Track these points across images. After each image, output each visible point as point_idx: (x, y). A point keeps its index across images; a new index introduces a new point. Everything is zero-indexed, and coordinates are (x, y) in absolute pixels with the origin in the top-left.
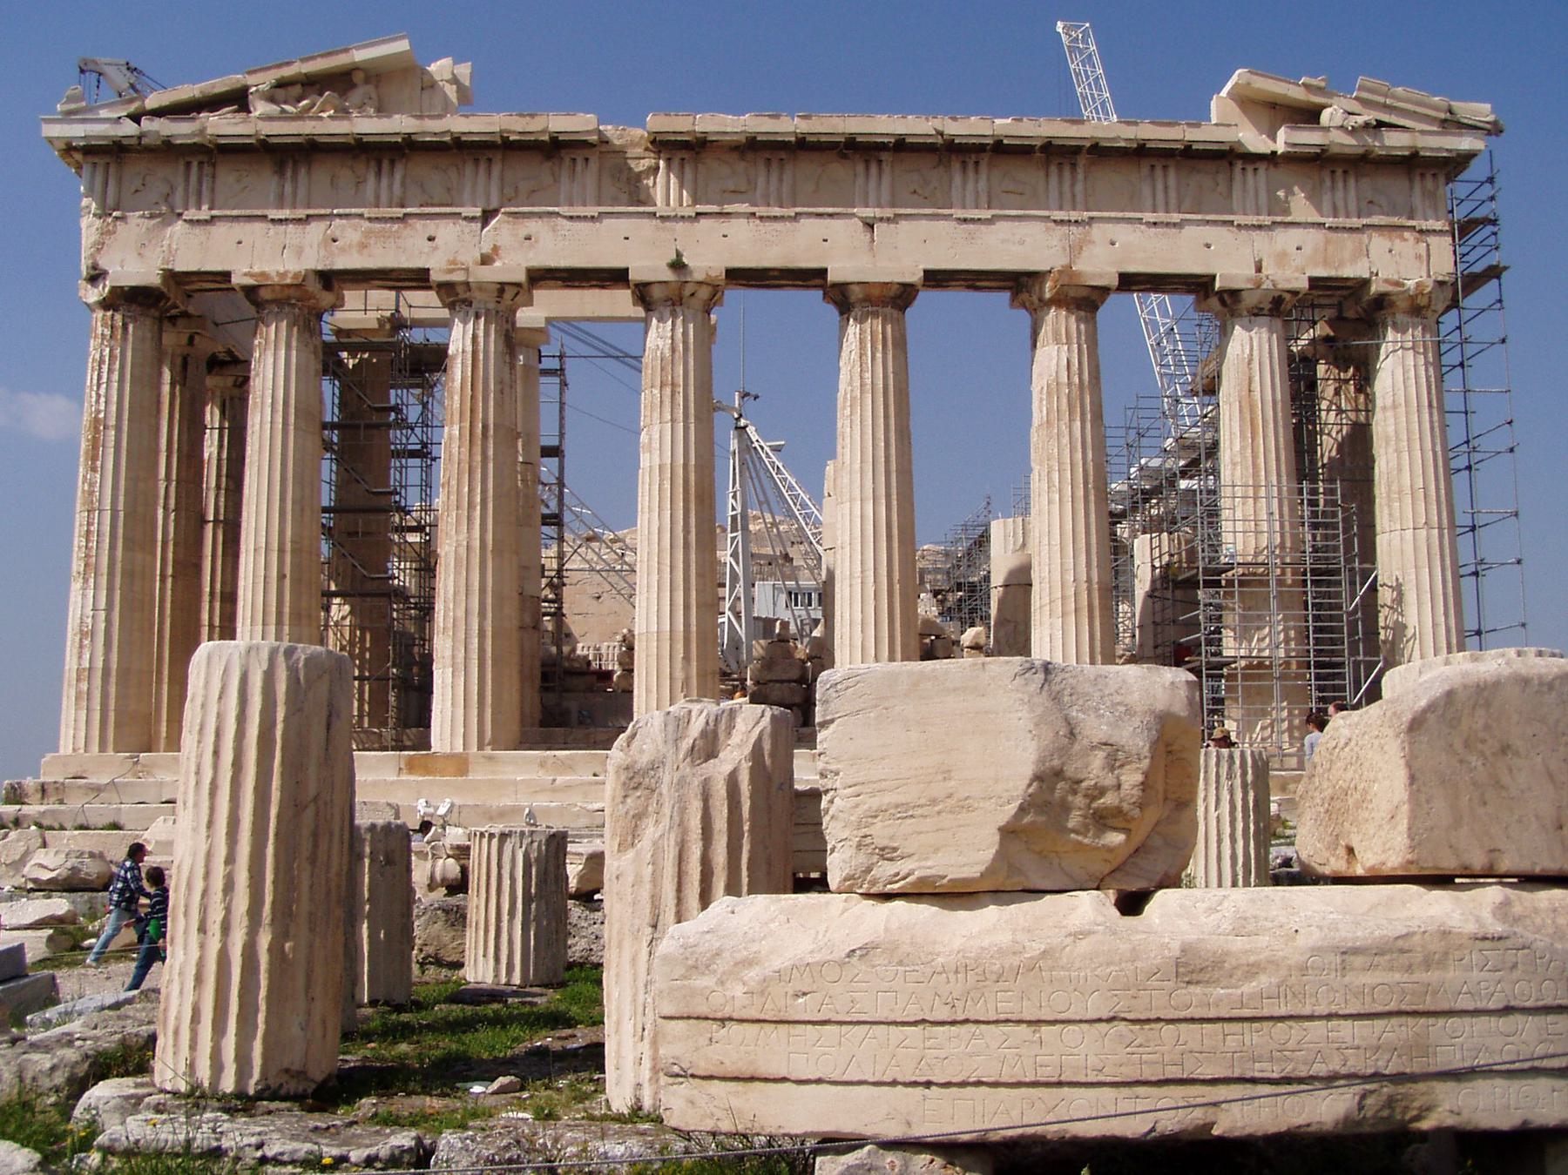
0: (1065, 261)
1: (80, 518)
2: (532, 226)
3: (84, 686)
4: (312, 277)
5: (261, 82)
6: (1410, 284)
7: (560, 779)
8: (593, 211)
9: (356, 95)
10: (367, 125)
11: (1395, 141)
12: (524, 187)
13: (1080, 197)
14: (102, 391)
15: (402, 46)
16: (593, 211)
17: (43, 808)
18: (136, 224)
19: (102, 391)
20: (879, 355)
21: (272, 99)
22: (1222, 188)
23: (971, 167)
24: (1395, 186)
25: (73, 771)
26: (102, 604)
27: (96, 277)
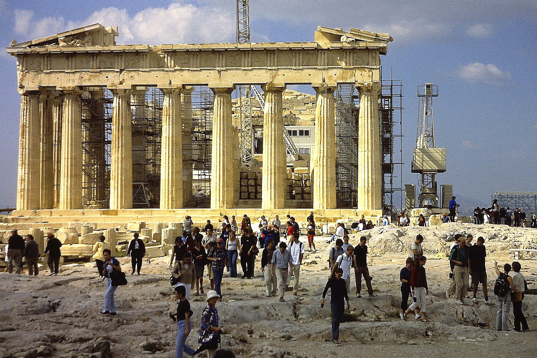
0: (271, 81)
1: (20, 150)
2: (133, 74)
3: (22, 193)
4: (77, 87)
5: (61, 38)
6: (366, 84)
7: (139, 216)
8: (148, 70)
9: (86, 39)
10: (89, 49)
11: (362, 45)
12: (131, 62)
13: (276, 63)
14: (25, 117)
15: (98, 26)
16: (148, 70)
17: (13, 224)
18: (31, 75)
19: (25, 117)
20: (222, 107)
21: (64, 42)
22: (315, 59)
23: (247, 54)
24: (364, 55)
25: (20, 214)
26: (26, 173)
27: (22, 87)
